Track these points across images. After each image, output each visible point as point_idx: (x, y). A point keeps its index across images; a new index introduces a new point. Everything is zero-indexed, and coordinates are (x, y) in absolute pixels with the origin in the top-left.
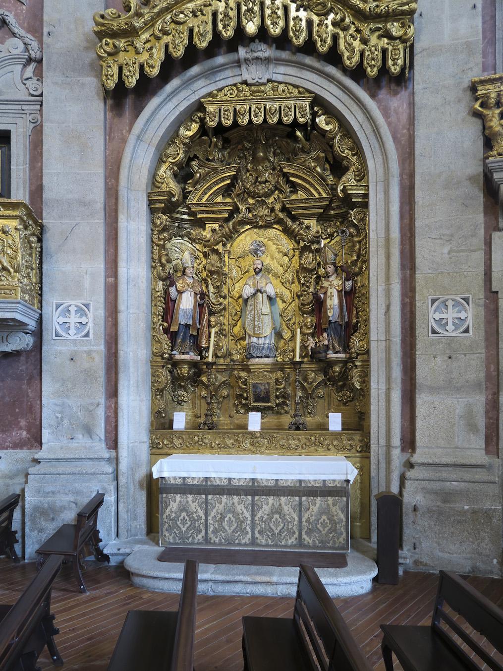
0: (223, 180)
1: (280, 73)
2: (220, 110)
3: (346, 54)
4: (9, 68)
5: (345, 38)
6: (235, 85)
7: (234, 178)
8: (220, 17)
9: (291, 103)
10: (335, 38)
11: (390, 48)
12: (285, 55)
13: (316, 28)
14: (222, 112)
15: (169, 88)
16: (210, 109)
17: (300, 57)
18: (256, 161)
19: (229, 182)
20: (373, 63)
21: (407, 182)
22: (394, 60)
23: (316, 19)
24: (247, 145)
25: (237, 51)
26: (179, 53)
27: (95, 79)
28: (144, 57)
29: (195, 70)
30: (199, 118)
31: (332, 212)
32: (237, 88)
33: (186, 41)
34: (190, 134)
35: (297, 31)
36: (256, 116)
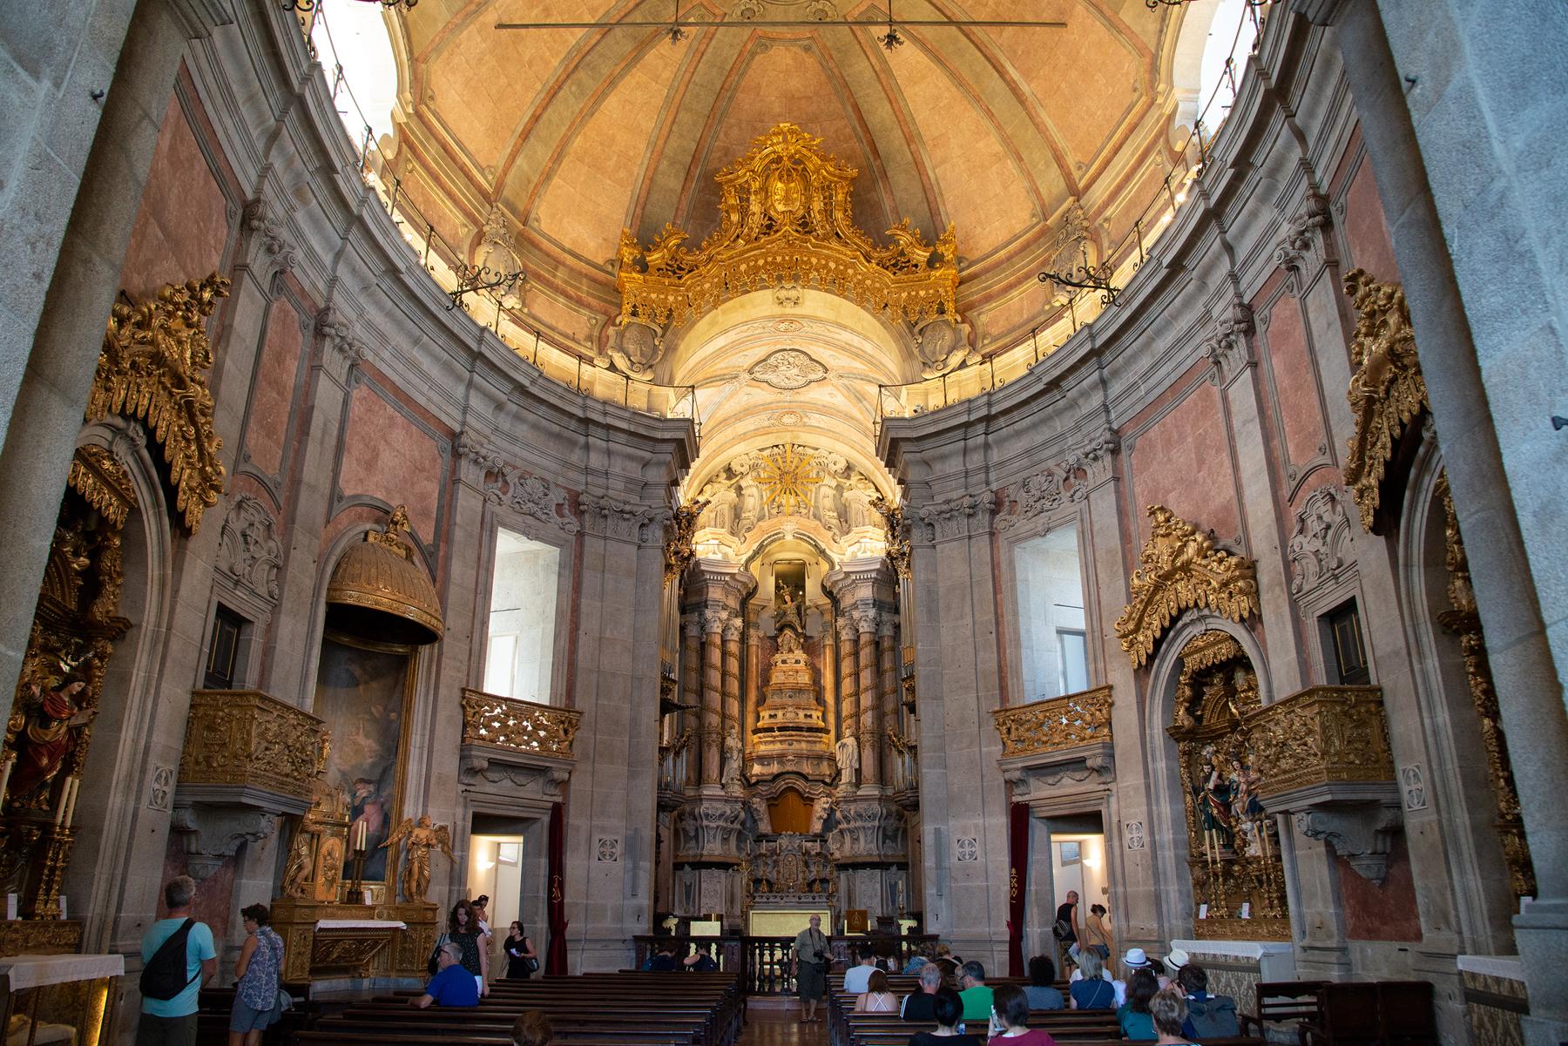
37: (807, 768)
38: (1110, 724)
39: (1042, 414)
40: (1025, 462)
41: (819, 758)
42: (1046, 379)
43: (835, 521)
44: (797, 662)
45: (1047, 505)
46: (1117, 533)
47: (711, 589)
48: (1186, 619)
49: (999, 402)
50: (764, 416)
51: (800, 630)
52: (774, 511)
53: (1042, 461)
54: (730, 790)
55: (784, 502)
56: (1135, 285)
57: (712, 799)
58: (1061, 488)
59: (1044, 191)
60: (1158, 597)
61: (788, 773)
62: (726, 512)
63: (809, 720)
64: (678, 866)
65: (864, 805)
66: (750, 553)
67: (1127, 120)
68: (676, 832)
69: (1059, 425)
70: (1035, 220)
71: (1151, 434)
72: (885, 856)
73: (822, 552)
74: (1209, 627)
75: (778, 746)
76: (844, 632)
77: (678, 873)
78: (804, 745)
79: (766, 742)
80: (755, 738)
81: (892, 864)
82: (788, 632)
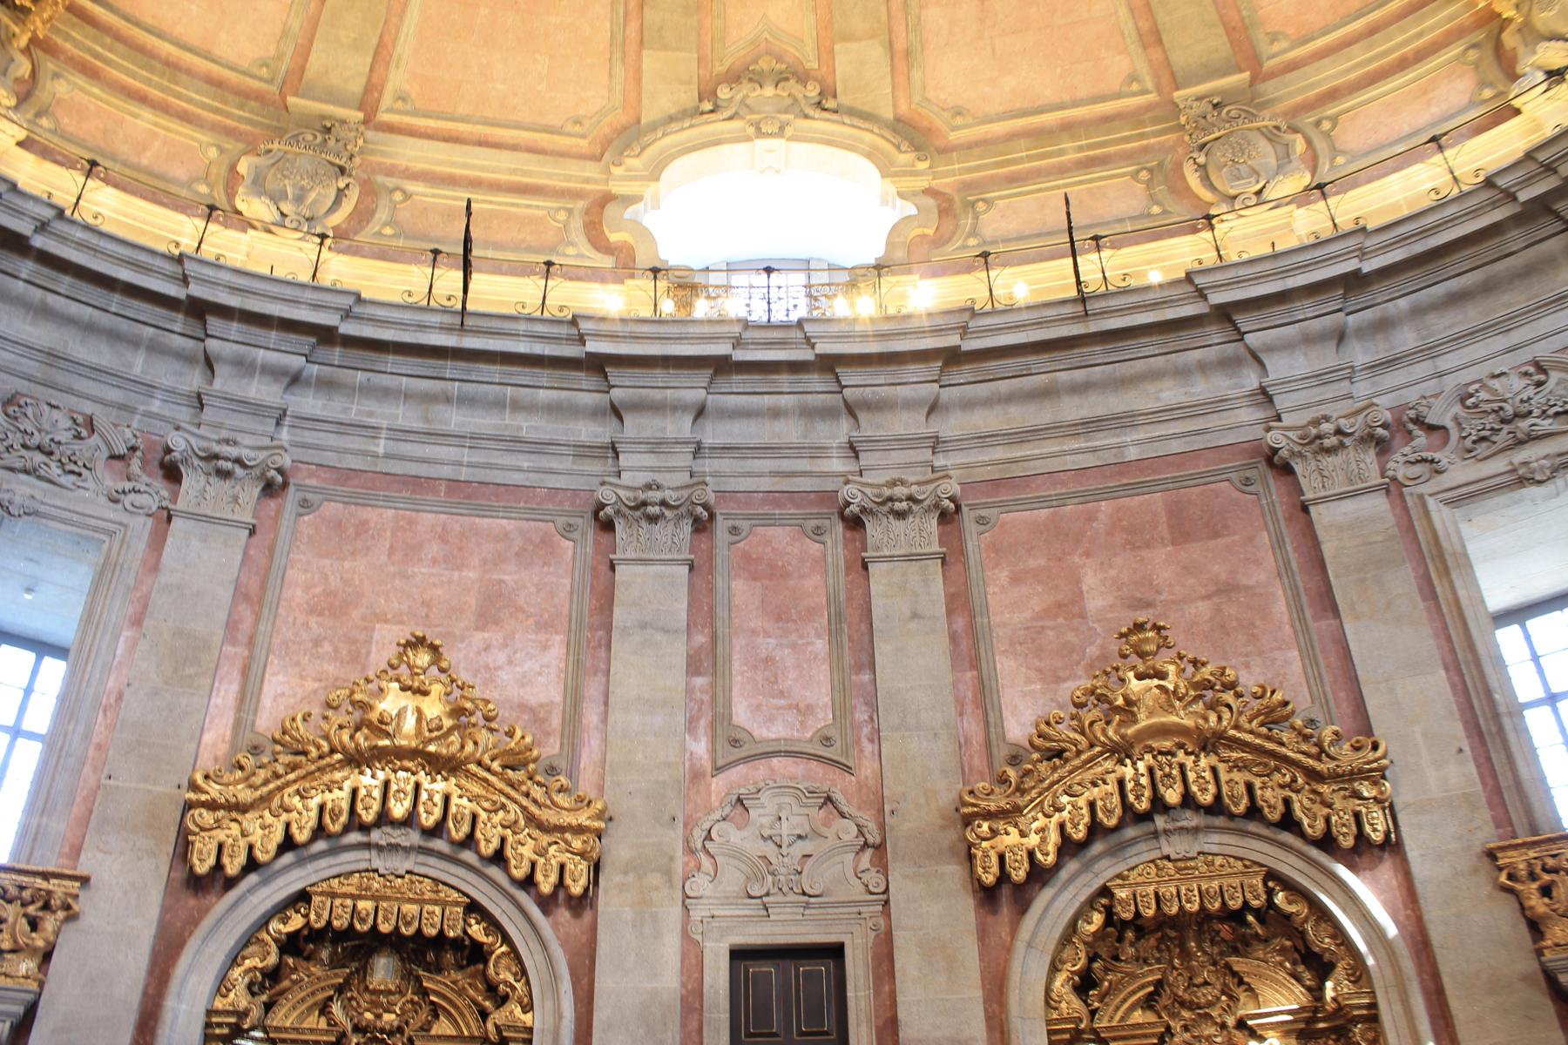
0: (1143, 987)
1: (1212, 842)
2: (1134, 895)
3: (1306, 821)
4: (838, 859)
5: (1300, 802)
6: (1153, 861)
7: (1159, 984)
8: (1130, 786)
9: (1235, 882)
10: (1287, 802)
11: (1364, 810)
12: (1220, 821)
13: (1259, 792)
14: (1139, 899)
15: (1064, 874)
16: (1122, 894)
17: (1241, 824)
18: (1186, 955)
19: (1151, 989)
20: (1345, 830)
21: (1431, 985)
22: (1372, 825)
23: (1257, 782)
24: (1172, 934)
25: (1153, 820)
26: (1079, 834)
27: (958, 867)
28: (1033, 840)
29: (1098, 847)
30: (1103, 906)
31: (1321, 1025)
32: (1156, 866)
33: (1087, 819)
34: (1092, 928)
35: (1235, 800)
36: (1189, 901)
38: (47, 956)
39: (124, 325)
40: (32, 367)
42: (196, 290)
45: (55, 471)
46: (222, 616)
48: (376, 836)
49: (63, 239)
53: (70, 391)
56: (507, 325)
58: (100, 465)
59: (316, 63)
60: (338, 775)
67: (538, 136)
69: (138, 364)
70: (264, 72)
71: (371, 515)
74: (417, 869)
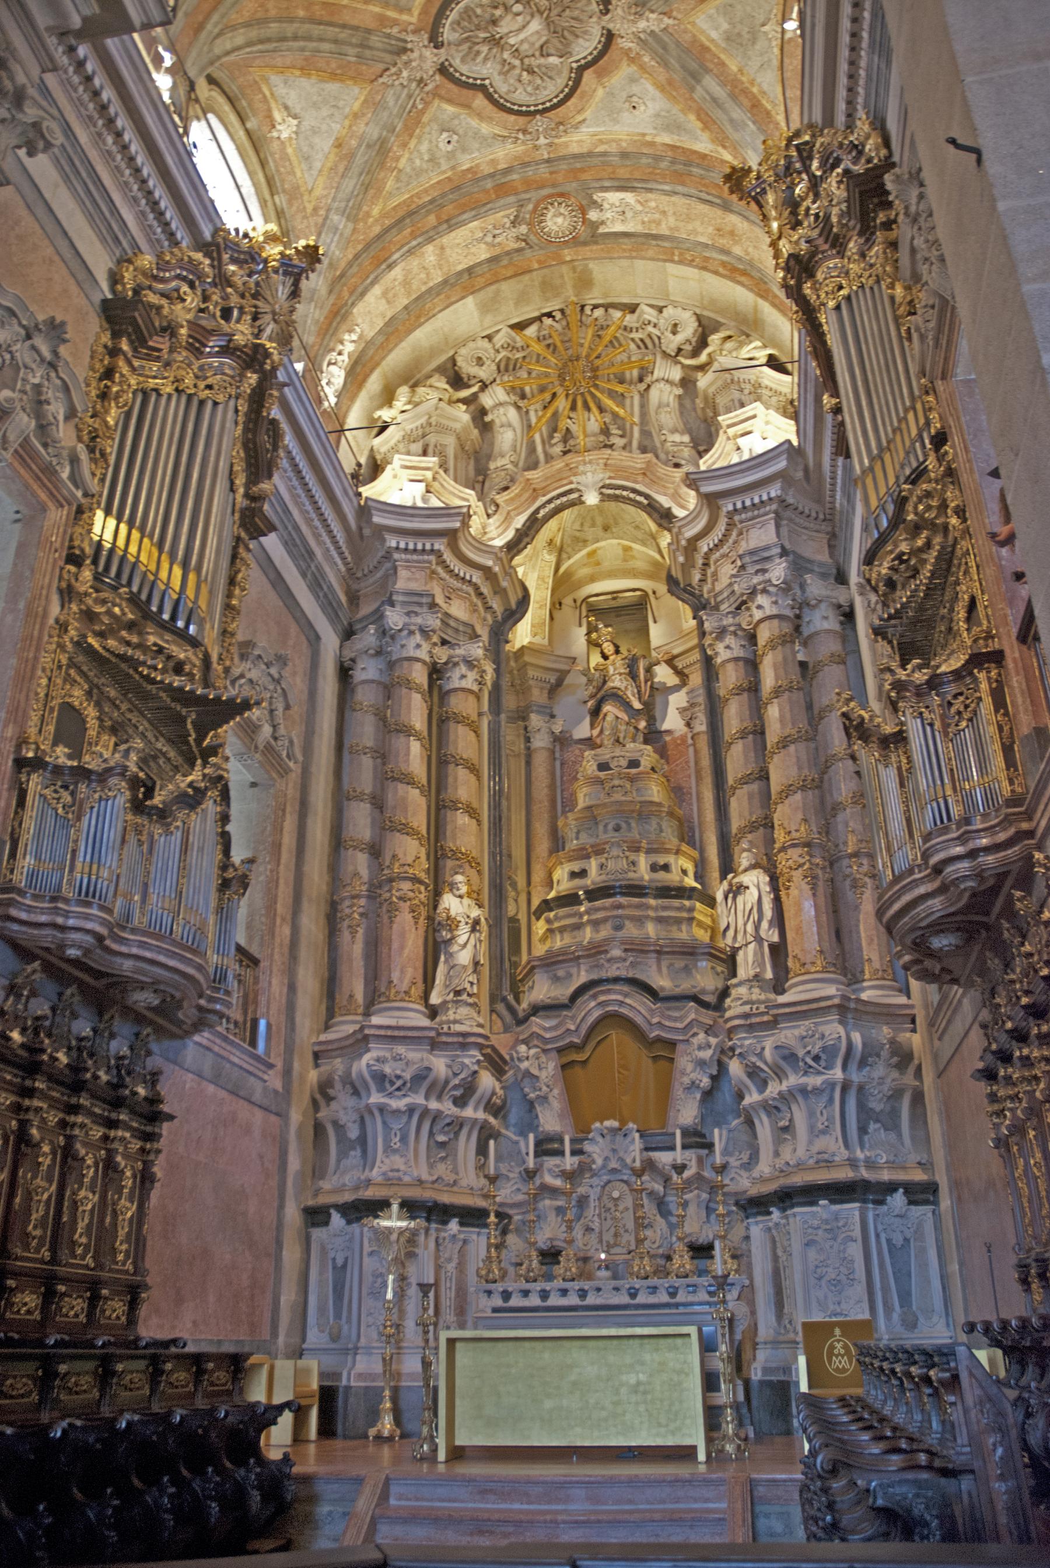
37: (662, 982)
41: (690, 951)
43: (687, 452)
44: (634, 764)
47: (402, 573)
50: (503, 216)
51: (637, 705)
52: (558, 449)
54: (451, 1015)
55: (574, 428)
57: (395, 1036)
61: (608, 981)
62: (451, 452)
63: (661, 875)
64: (316, 1216)
65: (804, 1027)
66: (510, 534)
68: (319, 1129)
72: (870, 1165)
73: (665, 517)
75: (588, 933)
76: (720, 647)
77: (318, 1234)
78: (651, 929)
79: (562, 930)
80: (540, 927)
81: (891, 1188)
82: (610, 709)
